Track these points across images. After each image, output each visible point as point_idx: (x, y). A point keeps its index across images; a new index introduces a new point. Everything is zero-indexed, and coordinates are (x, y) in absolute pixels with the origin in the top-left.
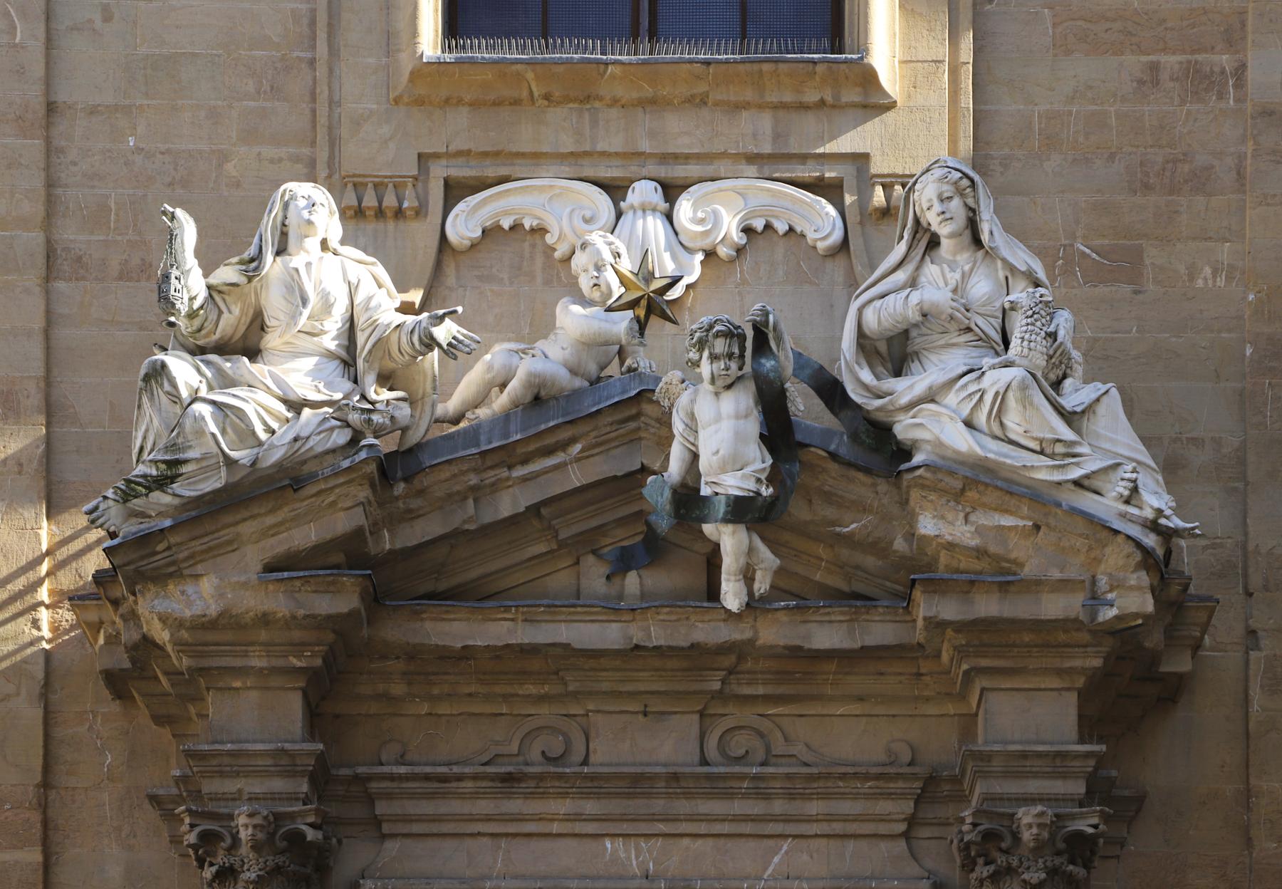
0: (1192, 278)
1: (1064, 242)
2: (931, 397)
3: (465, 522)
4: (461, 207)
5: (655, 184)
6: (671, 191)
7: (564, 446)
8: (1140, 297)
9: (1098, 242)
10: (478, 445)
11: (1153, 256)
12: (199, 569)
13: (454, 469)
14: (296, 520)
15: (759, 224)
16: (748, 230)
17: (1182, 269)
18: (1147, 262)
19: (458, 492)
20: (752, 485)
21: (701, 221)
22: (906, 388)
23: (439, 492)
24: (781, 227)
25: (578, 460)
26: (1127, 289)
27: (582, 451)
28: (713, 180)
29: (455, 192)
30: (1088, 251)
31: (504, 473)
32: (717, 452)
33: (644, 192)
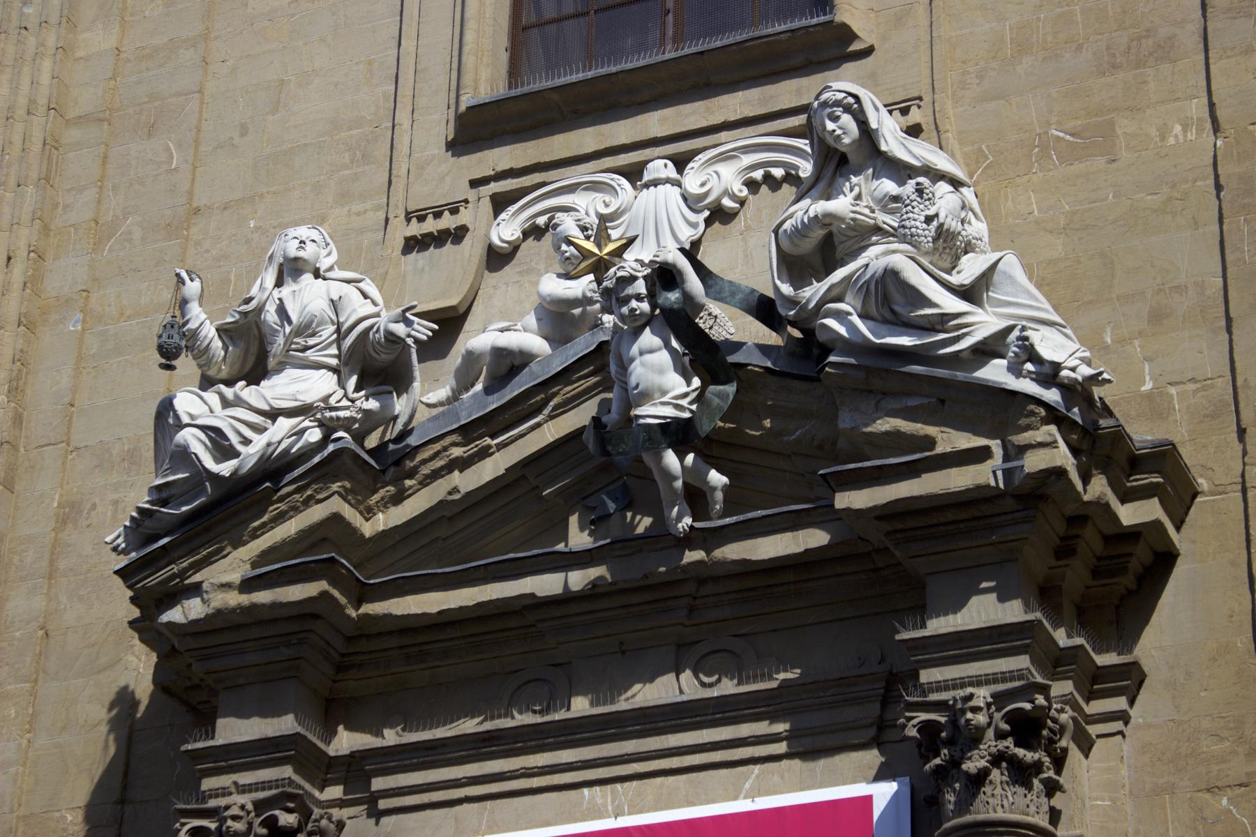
0: (1163, 138)
1: (1038, 131)
2: (836, 295)
3: (450, 493)
4: (503, 216)
5: (663, 161)
6: (681, 163)
7: (538, 410)
8: (1114, 165)
9: (1071, 125)
10: (459, 420)
11: (1124, 125)
12: (197, 578)
13: (437, 447)
14: (281, 518)
15: (758, 175)
16: (752, 185)
17: (1153, 132)
18: (1119, 131)
19: (442, 468)
20: (669, 412)
21: (703, 185)
22: (813, 292)
23: (425, 470)
24: (778, 172)
25: (551, 417)
26: (1100, 162)
27: (554, 409)
28: (715, 146)
29: (500, 203)
30: (1061, 135)
31: (488, 441)
32: (637, 386)
33: (660, 168)
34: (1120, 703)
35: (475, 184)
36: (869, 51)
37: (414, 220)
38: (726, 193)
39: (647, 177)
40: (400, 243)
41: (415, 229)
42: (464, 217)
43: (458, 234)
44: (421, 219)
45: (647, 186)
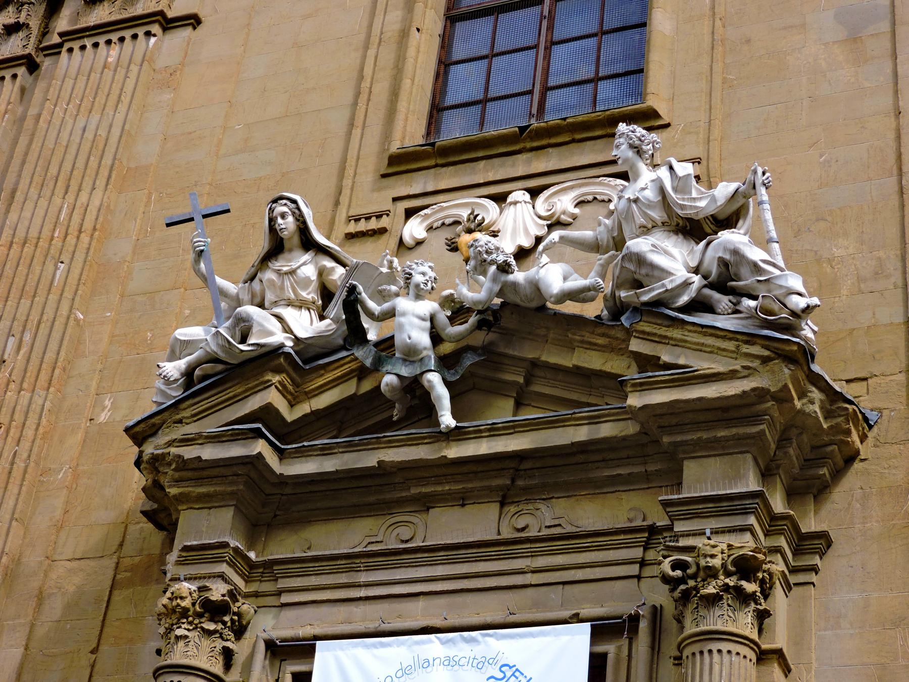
6: (534, 193)
29: (410, 213)
34: (816, 560)
35: (395, 200)
36: (668, 126)
37: (353, 222)
38: (564, 213)
39: (509, 200)
40: (341, 236)
41: (352, 228)
42: (384, 222)
43: (383, 231)
44: (357, 220)
45: (511, 204)
